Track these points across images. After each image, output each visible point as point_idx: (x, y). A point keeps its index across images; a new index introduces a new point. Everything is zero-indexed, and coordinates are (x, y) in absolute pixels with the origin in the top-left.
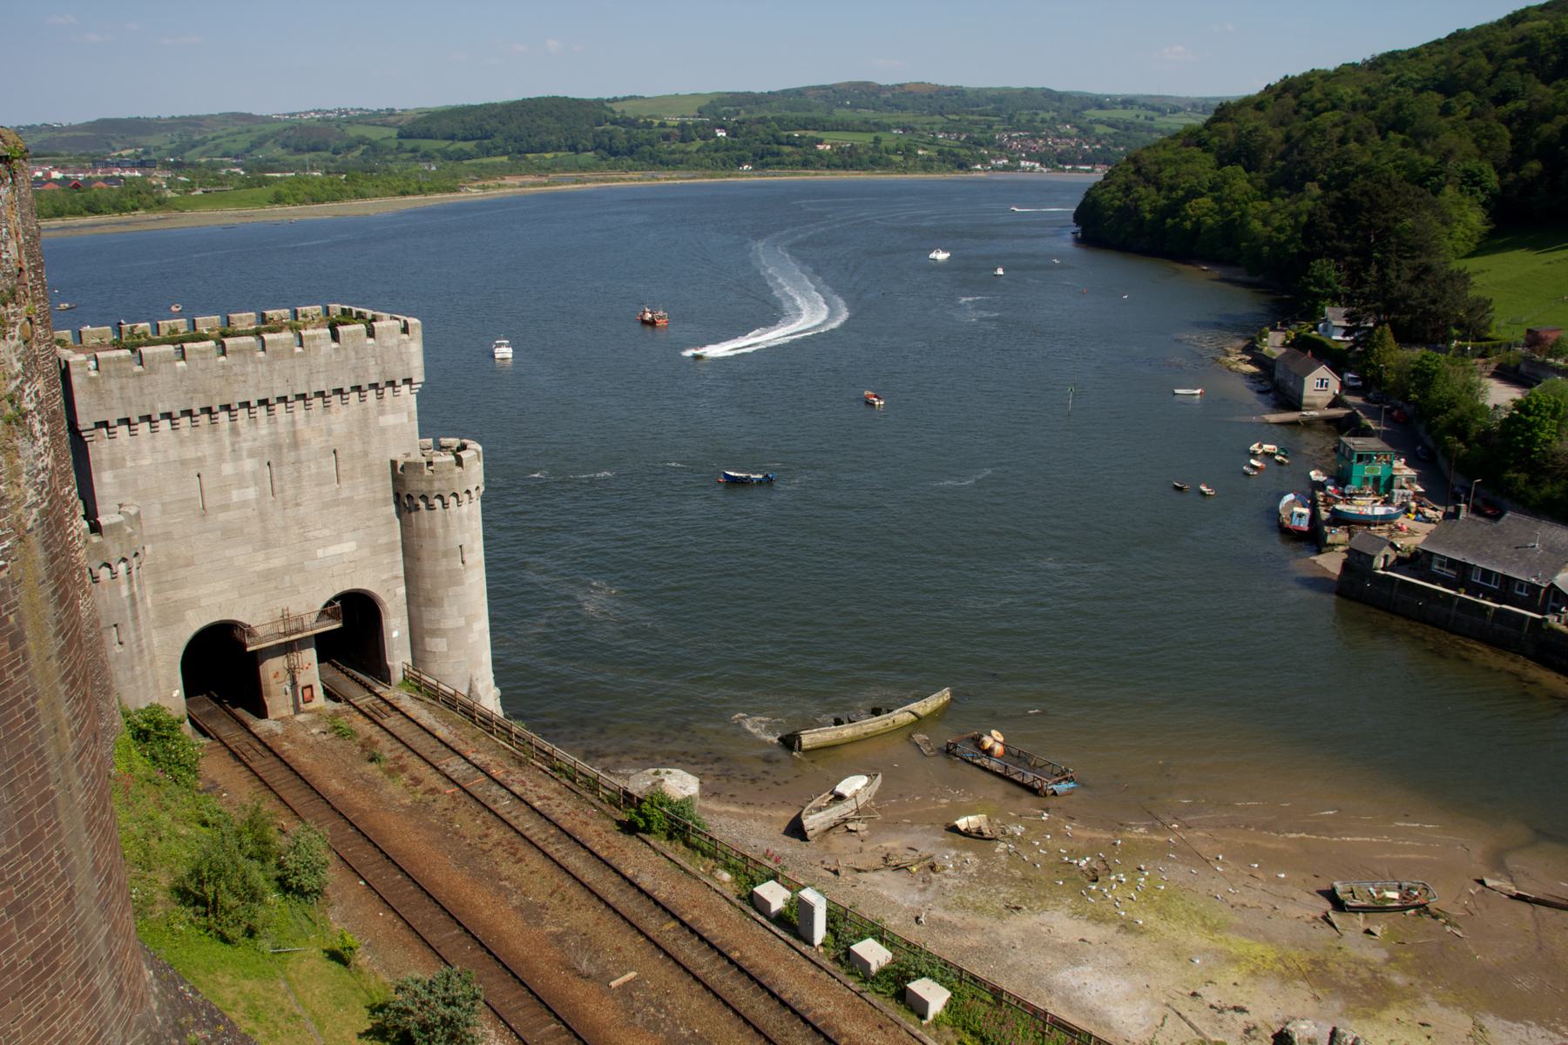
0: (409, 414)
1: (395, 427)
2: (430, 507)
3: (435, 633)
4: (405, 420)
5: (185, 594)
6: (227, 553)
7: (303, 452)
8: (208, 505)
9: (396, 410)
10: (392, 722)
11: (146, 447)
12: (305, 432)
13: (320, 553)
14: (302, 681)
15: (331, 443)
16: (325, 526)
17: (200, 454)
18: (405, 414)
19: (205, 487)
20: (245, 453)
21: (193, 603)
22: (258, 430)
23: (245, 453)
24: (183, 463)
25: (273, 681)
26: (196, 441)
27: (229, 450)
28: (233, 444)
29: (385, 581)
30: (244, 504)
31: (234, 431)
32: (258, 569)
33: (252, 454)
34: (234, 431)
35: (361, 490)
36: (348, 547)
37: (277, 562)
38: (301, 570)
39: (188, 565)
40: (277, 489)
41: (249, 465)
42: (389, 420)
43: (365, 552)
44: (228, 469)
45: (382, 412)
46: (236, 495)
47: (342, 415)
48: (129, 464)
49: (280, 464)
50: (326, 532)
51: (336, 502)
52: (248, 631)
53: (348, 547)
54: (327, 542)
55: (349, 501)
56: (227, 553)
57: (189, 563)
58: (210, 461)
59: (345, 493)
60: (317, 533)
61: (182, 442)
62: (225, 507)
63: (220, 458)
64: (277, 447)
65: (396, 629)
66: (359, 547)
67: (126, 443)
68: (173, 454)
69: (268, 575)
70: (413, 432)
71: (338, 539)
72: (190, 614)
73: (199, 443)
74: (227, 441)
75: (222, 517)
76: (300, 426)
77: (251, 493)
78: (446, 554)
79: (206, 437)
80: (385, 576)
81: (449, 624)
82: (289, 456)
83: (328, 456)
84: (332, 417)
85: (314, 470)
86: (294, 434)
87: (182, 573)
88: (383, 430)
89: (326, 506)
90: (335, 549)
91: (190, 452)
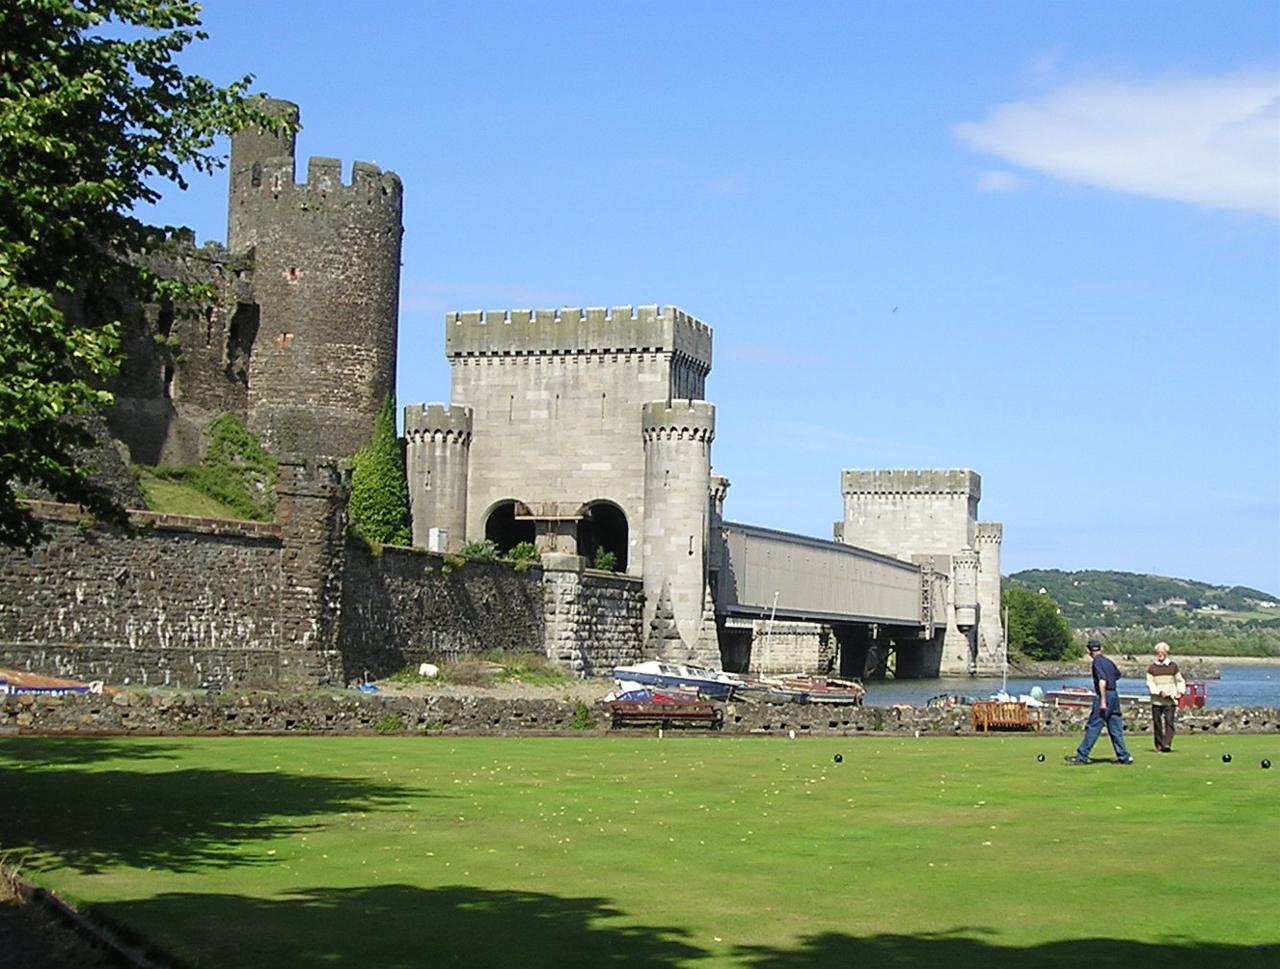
0: (663, 375)
1: (651, 383)
4: (659, 380)
5: (492, 475)
6: (523, 453)
9: (653, 372)
11: (484, 374)
12: (584, 379)
13: (584, 466)
15: (601, 389)
16: (590, 447)
17: (514, 383)
18: (659, 375)
20: (543, 387)
21: (496, 482)
22: (556, 369)
23: (543, 387)
27: (533, 382)
29: (629, 499)
30: (537, 421)
31: (539, 371)
32: (541, 468)
35: (620, 426)
36: (606, 467)
37: (553, 467)
39: (496, 456)
41: (545, 395)
42: (646, 377)
43: (617, 473)
44: (530, 395)
45: (641, 370)
46: (533, 414)
47: (611, 369)
48: (473, 383)
50: (591, 452)
51: (602, 432)
53: (606, 467)
54: (590, 459)
55: (610, 432)
56: (523, 453)
58: (519, 389)
60: (584, 452)
62: (525, 421)
63: (527, 387)
64: (564, 385)
66: (614, 469)
67: (473, 369)
69: (544, 474)
70: (665, 390)
72: (493, 489)
75: (523, 427)
76: (582, 373)
79: (520, 372)
80: (629, 496)
83: (599, 397)
84: (605, 370)
86: (576, 378)
87: (493, 460)
88: (641, 385)
89: (593, 433)
90: (595, 466)
91: (508, 381)
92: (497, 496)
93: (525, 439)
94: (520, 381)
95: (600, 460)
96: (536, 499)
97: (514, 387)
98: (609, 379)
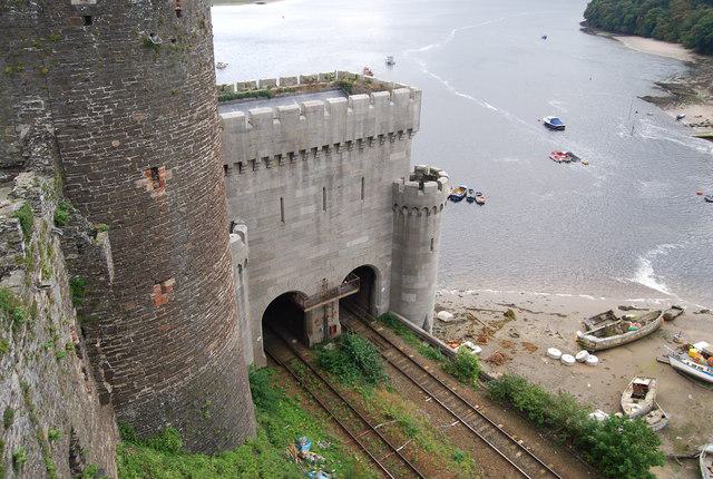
1: (398, 160)
2: (410, 215)
3: (409, 291)
7: (345, 179)
8: (286, 219)
10: (390, 354)
11: (250, 181)
14: (330, 324)
19: (285, 207)
21: (272, 283)
22: (320, 167)
24: (273, 191)
25: (314, 325)
26: (281, 175)
28: (304, 176)
30: (307, 217)
31: (306, 168)
33: (314, 184)
34: (306, 168)
36: (364, 239)
37: (324, 252)
38: (337, 256)
40: (327, 205)
41: (313, 190)
44: (299, 193)
46: (303, 211)
48: (239, 194)
49: (330, 189)
51: (361, 211)
52: (302, 295)
53: (364, 239)
54: (353, 237)
57: (272, 257)
59: (366, 205)
60: (347, 233)
61: (272, 176)
62: (296, 219)
64: (330, 177)
65: (383, 286)
68: (266, 186)
69: (316, 261)
71: (359, 235)
72: (270, 289)
73: (285, 179)
74: (300, 174)
77: (312, 209)
78: (424, 245)
81: (419, 286)
82: (336, 183)
85: (350, 191)
86: (340, 168)
88: (391, 164)
91: (277, 183)
92: (273, 294)
93: (296, 236)
94: (289, 182)
95: (361, 236)
96: (307, 286)
97: (283, 189)
98: (367, 163)
